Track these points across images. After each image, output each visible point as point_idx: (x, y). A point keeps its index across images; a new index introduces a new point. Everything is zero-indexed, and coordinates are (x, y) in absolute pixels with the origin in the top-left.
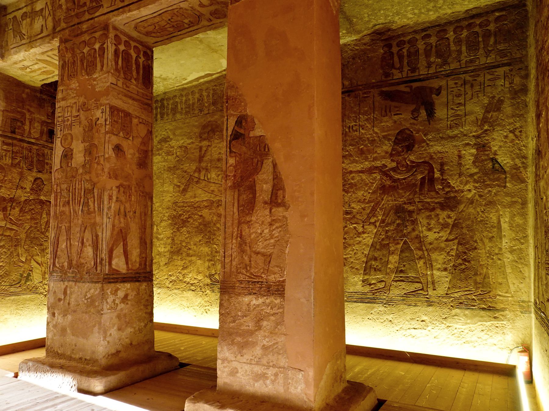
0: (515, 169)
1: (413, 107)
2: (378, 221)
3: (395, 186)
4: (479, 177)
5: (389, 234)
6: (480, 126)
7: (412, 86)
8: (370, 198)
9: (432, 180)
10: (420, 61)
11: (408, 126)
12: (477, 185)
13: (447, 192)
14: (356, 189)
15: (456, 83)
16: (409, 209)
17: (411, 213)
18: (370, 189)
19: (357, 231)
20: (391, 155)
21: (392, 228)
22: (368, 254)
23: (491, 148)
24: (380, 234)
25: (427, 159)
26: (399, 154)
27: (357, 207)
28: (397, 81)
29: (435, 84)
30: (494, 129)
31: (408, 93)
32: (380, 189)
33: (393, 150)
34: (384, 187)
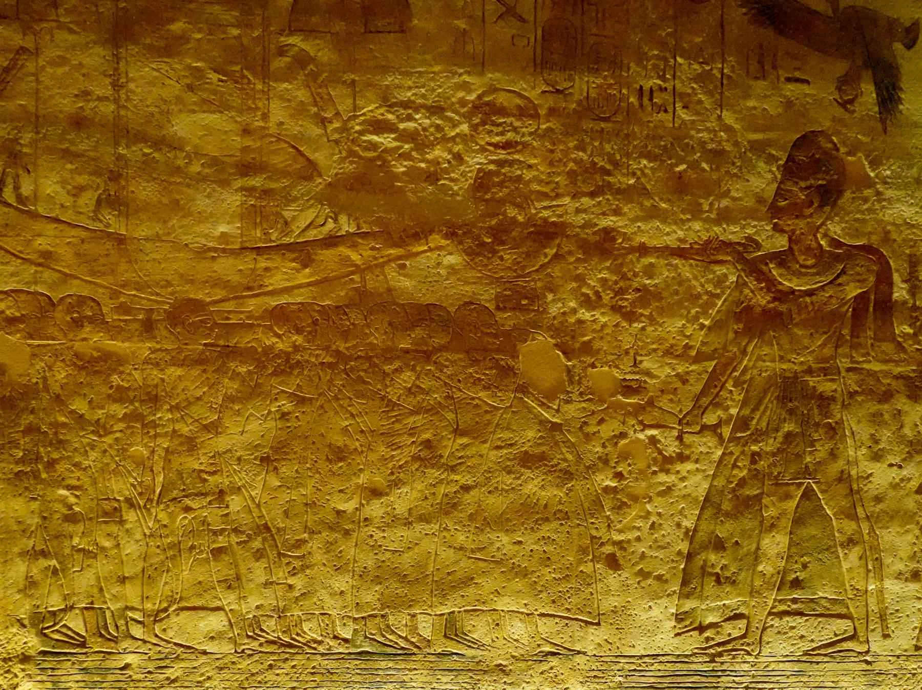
1: (841, 67)
2: (727, 422)
3: (781, 313)
5: (762, 464)
8: (703, 344)
11: (827, 124)
14: (661, 311)
18: (705, 313)
19: (660, 453)
20: (775, 211)
22: (695, 530)
24: (735, 466)
25: (875, 240)
26: (796, 211)
27: (661, 370)
32: (738, 317)
33: (779, 193)
34: (749, 309)
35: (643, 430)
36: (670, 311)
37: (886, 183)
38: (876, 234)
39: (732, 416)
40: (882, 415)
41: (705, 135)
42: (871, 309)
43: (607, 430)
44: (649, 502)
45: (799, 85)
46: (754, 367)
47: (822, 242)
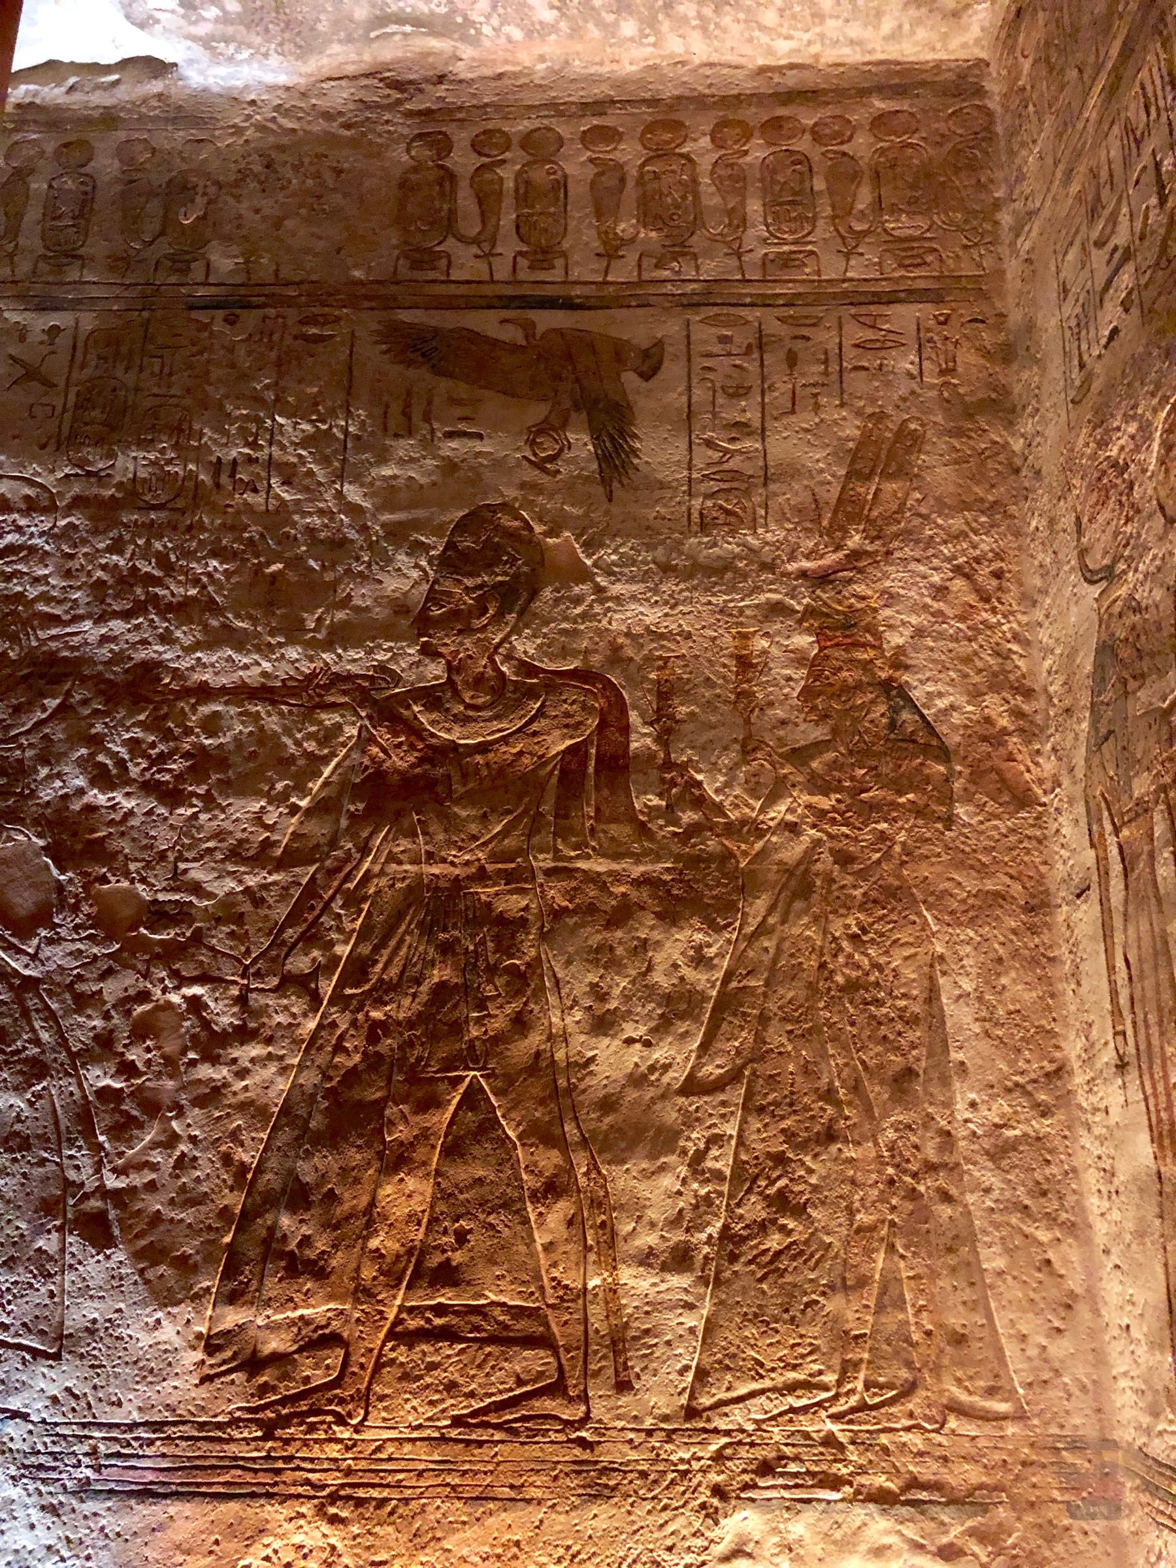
0: (984, 739)
1: (538, 412)
4: (834, 765)
5: (388, 1044)
6: (830, 532)
7: (533, 325)
9: (616, 765)
10: (572, 224)
11: (511, 493)
12: (825, 803)
13: (694, 830)
15: (724, 340)
16: (500, 907)
17: (508, 929)
21: (403, 1008)
23: (878, 636)
25: (596, 660)
26: (460, 621)
28: (462, 290)
29: (636, 328)
30: (889, 553)
31: (515, 348)
35: (177, 988)
36: (243, 787)
37: (611, 573)
38: (596, 651)
39: (340, 958)
40: (611, 949)
41: (316, 521)
42: (591, 770)
43: (112, 990)
44: (176, 1117)
45: (466, 440)
46: (382, 873)
47: (504, 669)
